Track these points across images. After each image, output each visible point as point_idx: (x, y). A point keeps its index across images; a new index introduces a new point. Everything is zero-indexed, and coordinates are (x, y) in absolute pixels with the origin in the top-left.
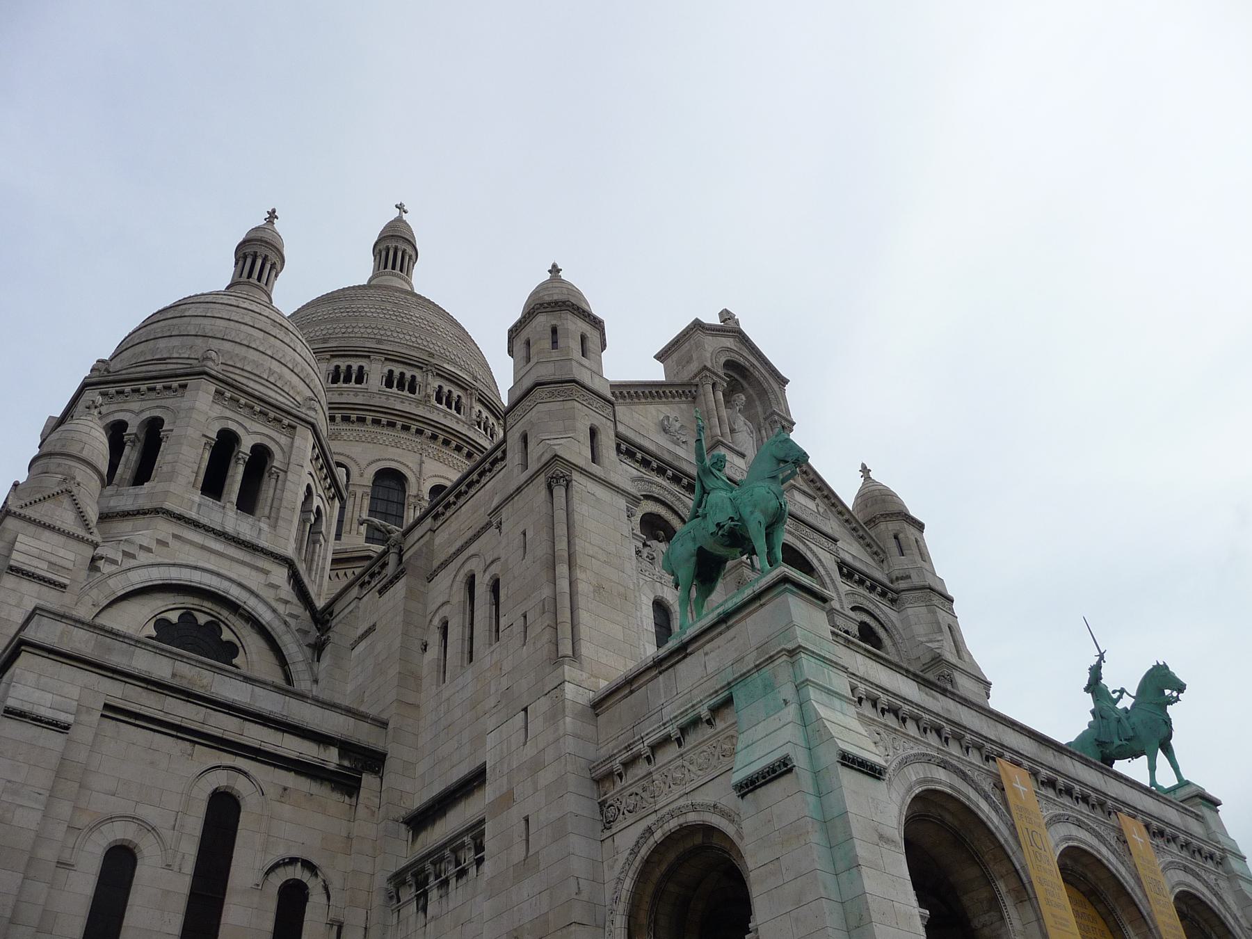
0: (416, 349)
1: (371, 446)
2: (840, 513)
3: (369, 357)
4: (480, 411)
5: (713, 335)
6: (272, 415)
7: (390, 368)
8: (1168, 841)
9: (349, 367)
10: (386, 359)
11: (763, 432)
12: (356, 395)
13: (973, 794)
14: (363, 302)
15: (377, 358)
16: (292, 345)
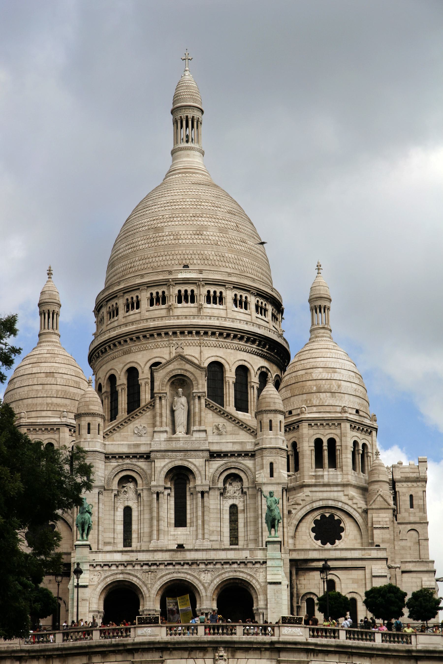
0: (161, 273)
1: (145, 352)
2: (235, 420)
3: (139, 289)
4: (209, 292)
5: (163, 369)
6: (49, 429)
7: (150, 292)
8: (231, 565)
9: (132, 298)
10: (148, 287)
11: (192, 401)
12: (133, 325)
13: (131, 577)
14: (138, 235)
15: (143, 288)
16: (55, 383)
